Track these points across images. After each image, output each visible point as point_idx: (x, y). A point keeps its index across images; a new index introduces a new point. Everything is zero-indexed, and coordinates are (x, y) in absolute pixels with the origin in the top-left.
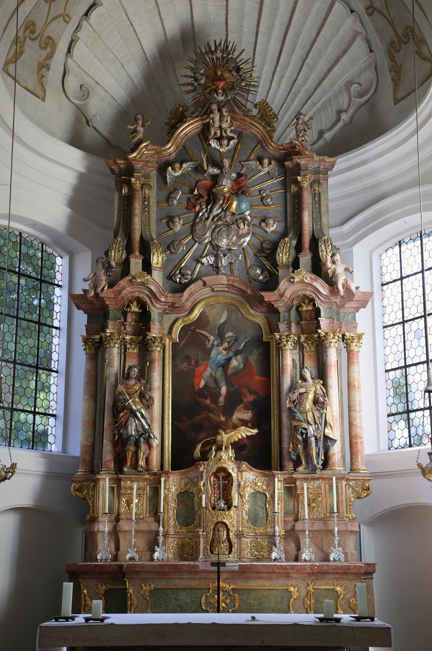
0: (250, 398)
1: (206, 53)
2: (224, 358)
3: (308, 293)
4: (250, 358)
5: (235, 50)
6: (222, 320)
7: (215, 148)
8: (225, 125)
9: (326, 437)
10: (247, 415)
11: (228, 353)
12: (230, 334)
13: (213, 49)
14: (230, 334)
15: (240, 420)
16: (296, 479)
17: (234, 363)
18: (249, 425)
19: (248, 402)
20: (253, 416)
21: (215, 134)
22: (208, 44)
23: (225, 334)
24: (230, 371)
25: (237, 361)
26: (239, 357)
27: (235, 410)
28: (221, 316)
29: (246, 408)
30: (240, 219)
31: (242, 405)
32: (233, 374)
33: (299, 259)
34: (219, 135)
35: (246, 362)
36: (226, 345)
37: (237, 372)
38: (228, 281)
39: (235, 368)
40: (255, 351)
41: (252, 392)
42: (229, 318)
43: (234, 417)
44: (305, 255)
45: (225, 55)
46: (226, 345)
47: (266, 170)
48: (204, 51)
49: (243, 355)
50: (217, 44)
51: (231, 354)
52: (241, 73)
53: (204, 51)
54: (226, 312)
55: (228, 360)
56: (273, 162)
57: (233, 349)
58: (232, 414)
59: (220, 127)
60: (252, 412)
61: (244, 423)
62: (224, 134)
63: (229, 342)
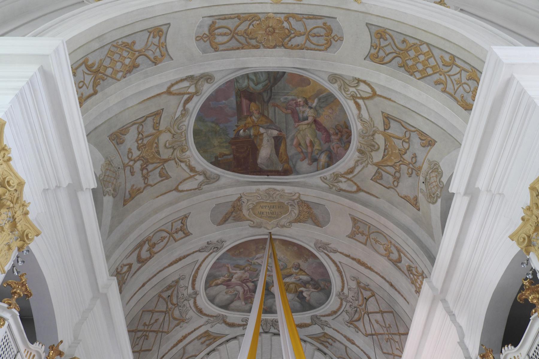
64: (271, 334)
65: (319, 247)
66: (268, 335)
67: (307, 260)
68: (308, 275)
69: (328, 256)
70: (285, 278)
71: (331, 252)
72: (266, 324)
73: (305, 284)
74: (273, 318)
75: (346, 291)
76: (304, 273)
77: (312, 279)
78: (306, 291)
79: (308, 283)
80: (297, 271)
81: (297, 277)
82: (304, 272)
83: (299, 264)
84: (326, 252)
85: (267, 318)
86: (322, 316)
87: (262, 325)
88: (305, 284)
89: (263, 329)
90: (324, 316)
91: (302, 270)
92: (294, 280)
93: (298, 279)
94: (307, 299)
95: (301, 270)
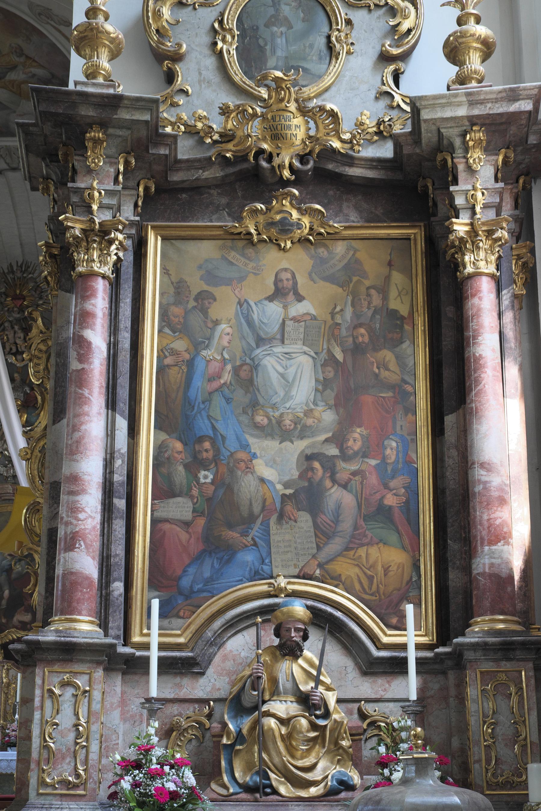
1: (9, 273)
5: (36, 270)
8: (18, 341)
21: (11, 349)
22: (11, 264)
34: (14, 350)
45: (25, 275)
48: (6, 271)
50: (19, 265)
52: (38, 292)
53: (6, 271)
59: (16, 343)
62: (20, 350)
65: (40, 14)
68: (43, 67)
69: (60, 31)
70: (7, 73)
71: (60, 24)
76: (34, 64)
77: (53, 76)
82: (34, 61)
83: (19, 45)
84: (52, 23)
85: (8, 144)
87: (3, 156)
89: (6, 163)
91: (31, 58)
92: (24, 76)
93: (30, 75)
95: (28, 57)
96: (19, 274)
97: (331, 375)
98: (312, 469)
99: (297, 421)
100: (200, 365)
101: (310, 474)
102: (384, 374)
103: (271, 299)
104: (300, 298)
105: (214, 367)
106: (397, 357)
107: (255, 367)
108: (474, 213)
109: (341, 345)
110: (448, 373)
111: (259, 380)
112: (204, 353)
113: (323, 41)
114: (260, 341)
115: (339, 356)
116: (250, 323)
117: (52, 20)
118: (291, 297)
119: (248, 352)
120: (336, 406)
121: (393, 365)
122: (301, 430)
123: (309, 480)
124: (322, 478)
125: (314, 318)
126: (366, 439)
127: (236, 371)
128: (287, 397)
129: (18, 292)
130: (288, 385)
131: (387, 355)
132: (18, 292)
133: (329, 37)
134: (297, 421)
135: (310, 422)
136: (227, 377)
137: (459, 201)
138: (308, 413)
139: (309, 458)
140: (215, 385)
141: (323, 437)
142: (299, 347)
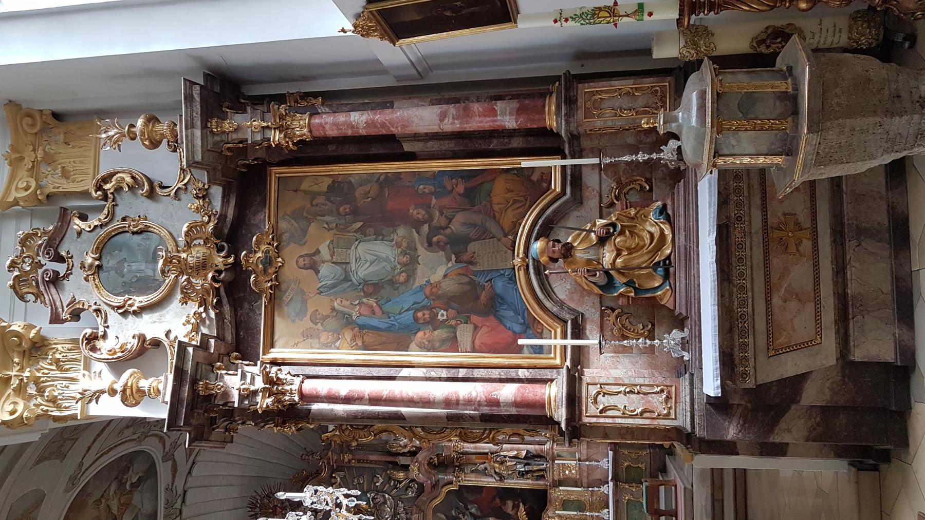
0: (498, 500)
2: (470, 517)
3: (426, 462)
4: (470, 499)
6: (444, 517)
7: (323, 516)
9: (526, 458)
10: (510, 503)
11: (467, 515)
12: (453, 512)
13: (254, 513)
14: (453, 512)
15: (513, 509)
16: (553, 480)
17: (473, 511)
18: (516, 503)
19: (500, 503)
20: (510, 499)
23: (453, 516)
24: (479, 514)
25: (472, 508)
26: (469, 507)
27: (505, 512)
28: (440, 518)
29: (505, 504)
30: (372, 501)
31: (503, 507)
32: (481, 512)
33: (402, 465)
35: (472, 502)
36: (461, 516)
37: (479, 509)
38: (416, 513)
39: (477, 510)
40: (465, 495)
41: (494, 499)
42: (442, 513)
43: (511, 513)
44: (399, 460)
46: (461, 516)
47: (339, 479)
49: (468, 504)
51: (467, 512)
54: (438, 514)
55: (471, 514)
56: (334, 475)
57: (464, 510)
58: (510, 515)
60: (507, 500)
61: (516, 507)
63: (459, 514)
64: (183, 506)
66: (184, 510)
67: (90, 494)
69: (87, 470)
71: (81, 469)
72: (169, 515)
73: (121, 484)
74: (163, 508)
75: (135, 437)
77: (116, 478)
78: (131, 480)
79: (120, 481)
80: (104, 501)
81: (112, 497)
86: (164, 451)
88: (121, 484)
90: (164, 448)
94: (140, 475)
96: (258, 510)
97: (372, 230)
98: (438, 242)
99: (404, 253)
100: (362, 320)
101: (441, 244)
102: (372, 194)
103: (317, 272)
104: (318, 252)
105: (365, 311)
106: (361, 186)
107: (365, 282)
108: (268, 127)
109: (351, 223)
110: (375, 150)
111: (375, 280)
112: (354, 318)
113: (136, 237)
114: (347, 279)
115: (359, 224)
116: (334, 286)
117: (78, 475)
118: (316, 258)
119: (354, 287)
120: (394, 227)
121: (366, 188)
122: (411, 250)
123: (446, 244)
124: (444, 235)
125: (332, 242)
126: (418, 206)
127: (368, 295)
128: (387, 260)
129: (271, 511)
130: (378, 259)
131: (359, 192)
132: (271, 511)
133: (134, 233)
134: (404, 253)
135: (405, 244)
136: (372, 302)
137: (258, 137)
138: (398, 245)
139: (430, 244)
140: (377, 310)
141: (416, 235)
142: (352, 252)
